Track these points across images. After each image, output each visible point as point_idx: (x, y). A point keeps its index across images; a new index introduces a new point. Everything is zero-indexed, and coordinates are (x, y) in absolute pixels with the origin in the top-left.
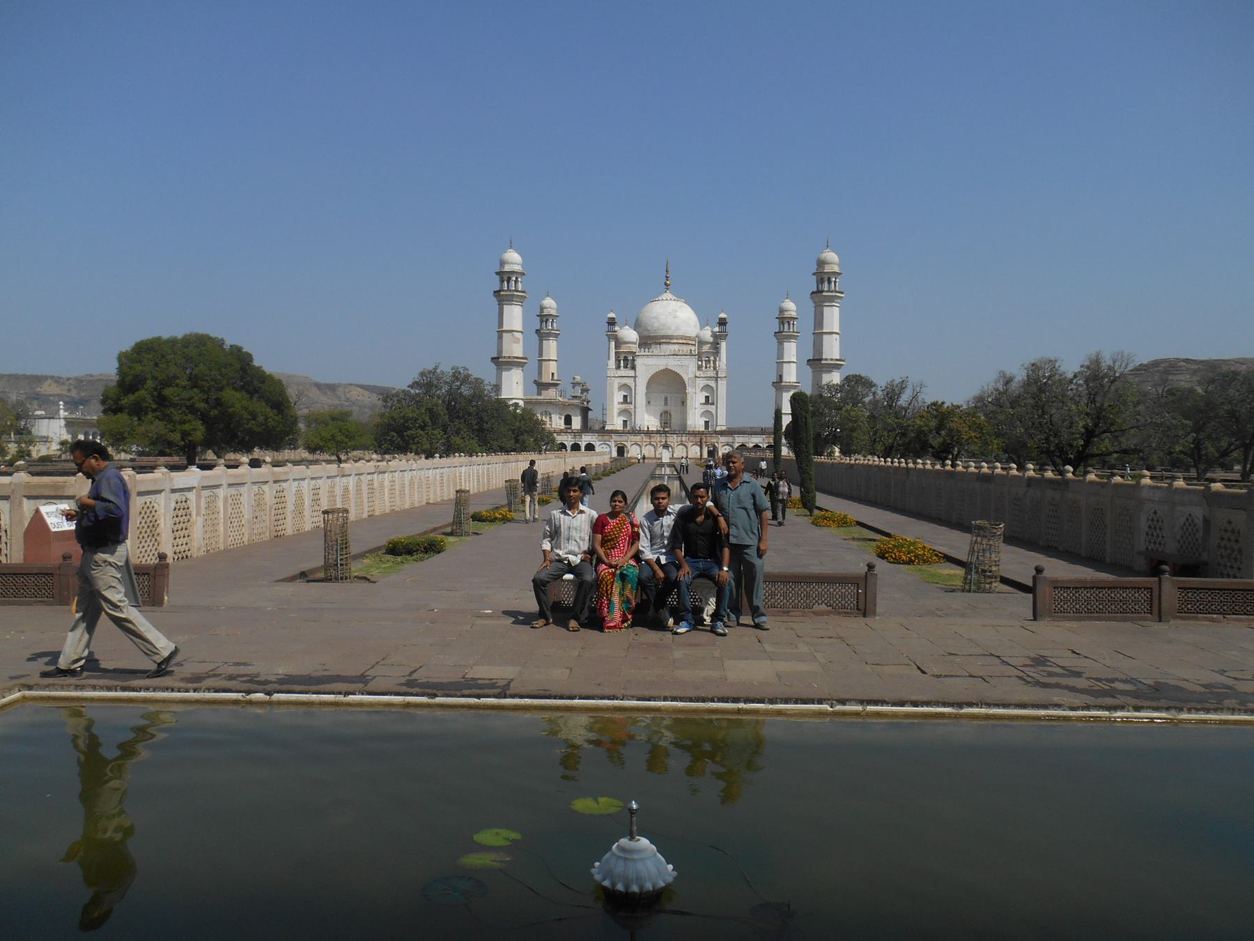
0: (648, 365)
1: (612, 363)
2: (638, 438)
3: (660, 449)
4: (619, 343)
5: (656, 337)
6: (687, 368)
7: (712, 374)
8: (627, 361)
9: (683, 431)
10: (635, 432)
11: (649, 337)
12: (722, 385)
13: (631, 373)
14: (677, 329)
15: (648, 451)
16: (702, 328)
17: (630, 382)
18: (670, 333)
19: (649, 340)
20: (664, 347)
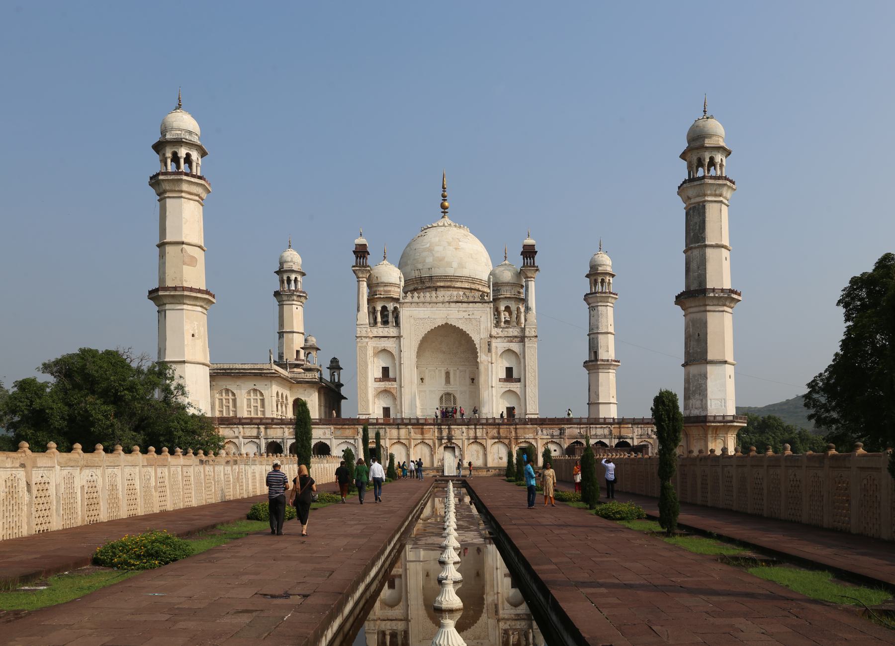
0: (419, 317)
1: (364, 315)
2: (403, 432)
3: (440, 451)
4: (372, 285)
5: (431, 278)
6: (478, 322)
7: (514, 331)
8: (386, 315)
9: (475, 422)
10: (400, 423)
11: (421, 280)
12: (532, 348)
13: (391, 331)
14: (461, 266)
15: (419, 453)
16: (496, 264)
17: (390, 345)
18: (450, 272)
19: (421, 284)
20: (441, 293)
